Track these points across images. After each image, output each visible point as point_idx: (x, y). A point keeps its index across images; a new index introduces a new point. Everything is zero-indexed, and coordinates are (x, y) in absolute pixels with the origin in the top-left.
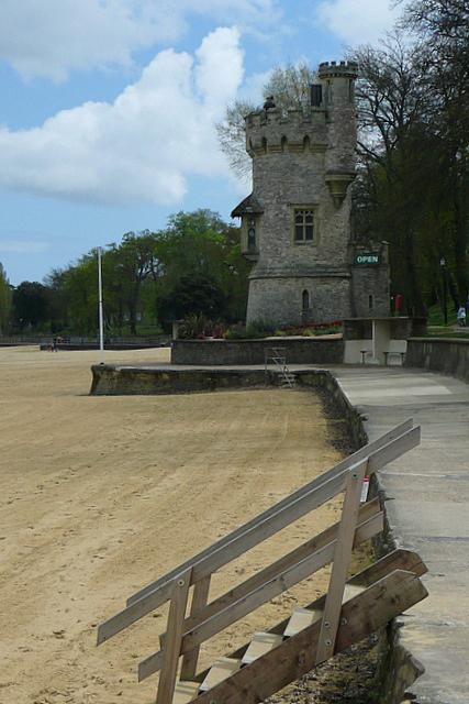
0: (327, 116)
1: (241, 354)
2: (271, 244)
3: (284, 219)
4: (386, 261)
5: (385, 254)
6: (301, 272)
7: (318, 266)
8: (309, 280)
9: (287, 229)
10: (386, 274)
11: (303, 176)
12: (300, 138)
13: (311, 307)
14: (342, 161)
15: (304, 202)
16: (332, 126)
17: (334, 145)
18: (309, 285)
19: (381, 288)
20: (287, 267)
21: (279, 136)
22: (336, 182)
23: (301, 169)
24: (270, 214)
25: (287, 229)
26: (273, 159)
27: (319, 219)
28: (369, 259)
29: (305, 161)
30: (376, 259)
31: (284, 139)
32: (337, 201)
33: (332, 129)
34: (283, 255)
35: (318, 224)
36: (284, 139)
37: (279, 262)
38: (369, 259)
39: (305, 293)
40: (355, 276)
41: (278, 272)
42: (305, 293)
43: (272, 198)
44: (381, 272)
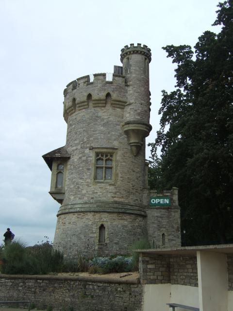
0: (126, 82)
1: (11, 293)
2: (73, 183)
3: (86, 161)
4: (177, 203)
5: (176, 198)
6: (101, 208)
7: (116, 202)
8: (106, 215)
9: (88, 169)
10: (177, 215)
11: (104, 125)
12: (103, 95)
13: (107, 241)
14: (139, 114)
15: (104, 146)
16: (130, 88)
17: (132, 101)
18: (106, 219)
19: (173, 227)
20: (86, 203)
21: (86, 94)
22: (133, 130)
23: (103, 120)
24: (75, 159)
25: (88, 169)
26: (80, 114)
27: (117, 161)
28: (161, 201)
29: (107, 113)
30: (167, 201)
31: (90, 96)
32: (134, 148)
33: (130, 90)
34: (84, 192)
35: (117, 166)
36: (90, 96)
37: (80, 198)
38: (161, 201)
39: (102, 227)
40: (149, 216)
41: (78, 208)
42: (102, 227)
43: (76, 145)
44: (173, 214)
